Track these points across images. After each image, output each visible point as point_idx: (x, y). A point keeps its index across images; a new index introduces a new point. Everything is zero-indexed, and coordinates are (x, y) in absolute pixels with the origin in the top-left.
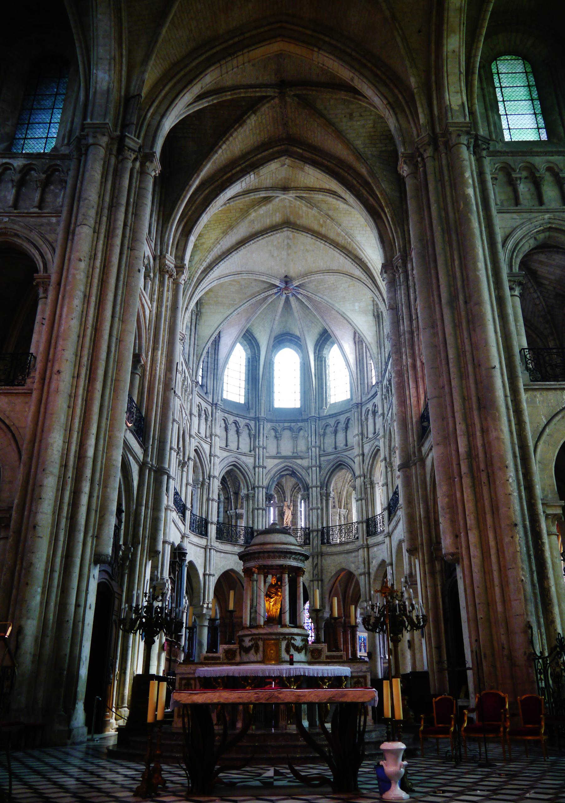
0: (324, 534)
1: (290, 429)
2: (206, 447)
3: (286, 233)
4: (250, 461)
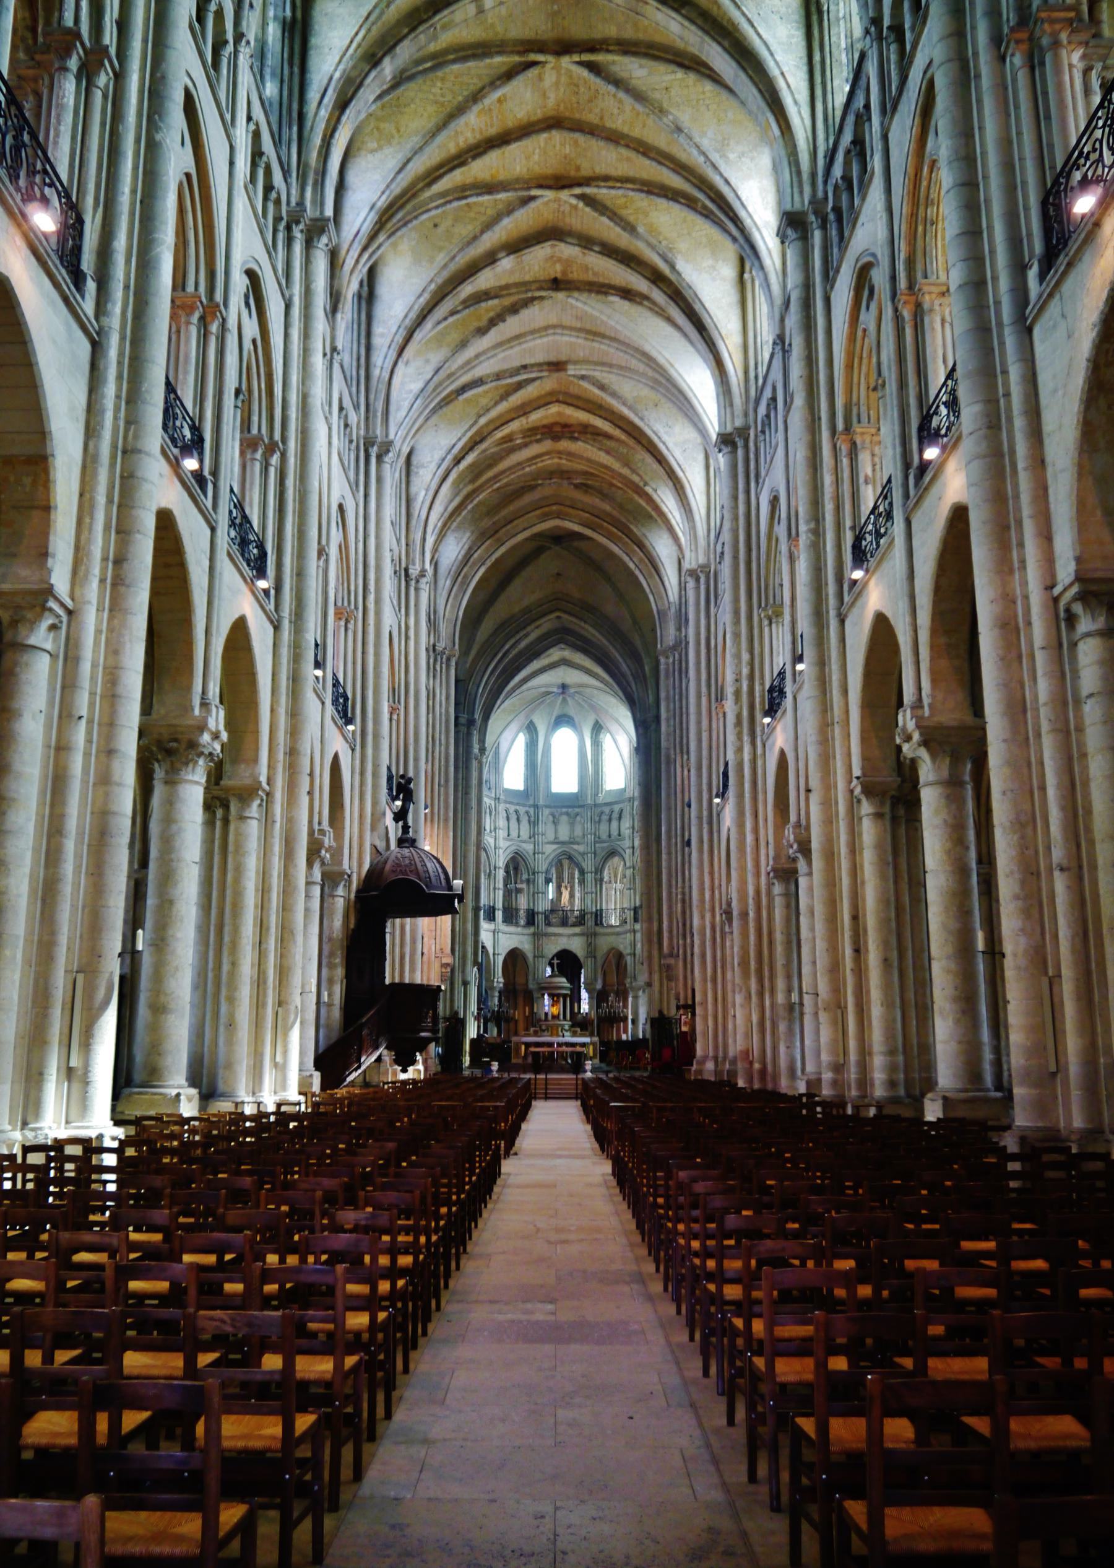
0: (598, 917)
1: (567, 814)
2: (491, 841)
3: (563, 668)
4: (529, 847)
